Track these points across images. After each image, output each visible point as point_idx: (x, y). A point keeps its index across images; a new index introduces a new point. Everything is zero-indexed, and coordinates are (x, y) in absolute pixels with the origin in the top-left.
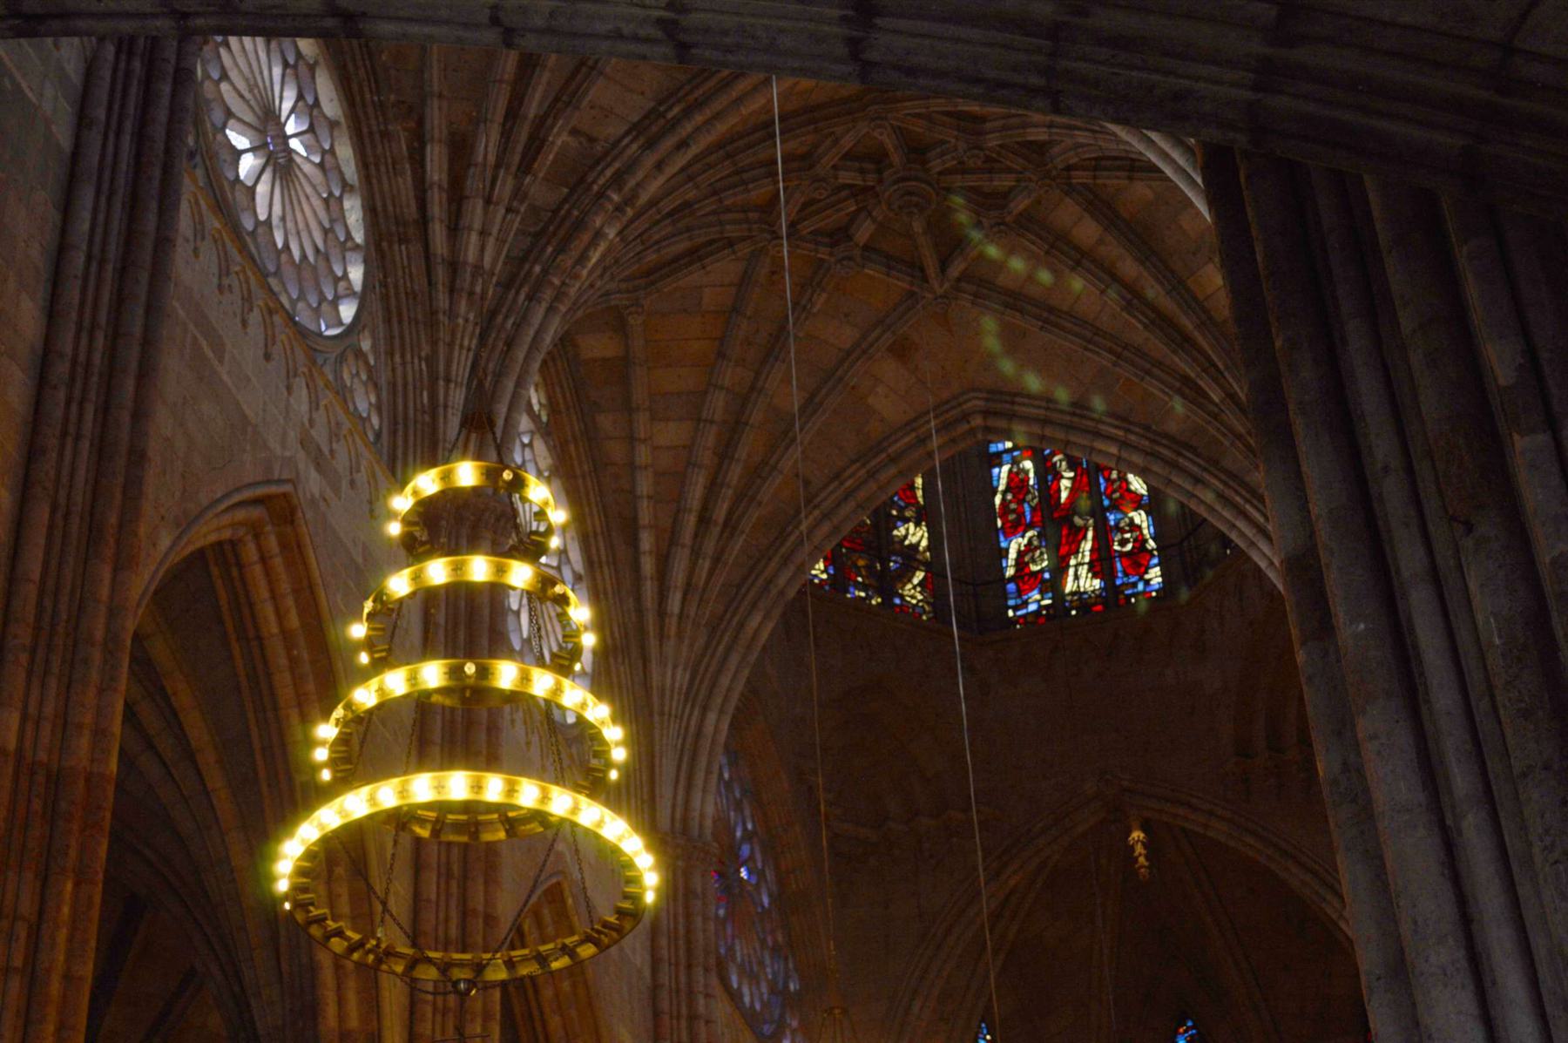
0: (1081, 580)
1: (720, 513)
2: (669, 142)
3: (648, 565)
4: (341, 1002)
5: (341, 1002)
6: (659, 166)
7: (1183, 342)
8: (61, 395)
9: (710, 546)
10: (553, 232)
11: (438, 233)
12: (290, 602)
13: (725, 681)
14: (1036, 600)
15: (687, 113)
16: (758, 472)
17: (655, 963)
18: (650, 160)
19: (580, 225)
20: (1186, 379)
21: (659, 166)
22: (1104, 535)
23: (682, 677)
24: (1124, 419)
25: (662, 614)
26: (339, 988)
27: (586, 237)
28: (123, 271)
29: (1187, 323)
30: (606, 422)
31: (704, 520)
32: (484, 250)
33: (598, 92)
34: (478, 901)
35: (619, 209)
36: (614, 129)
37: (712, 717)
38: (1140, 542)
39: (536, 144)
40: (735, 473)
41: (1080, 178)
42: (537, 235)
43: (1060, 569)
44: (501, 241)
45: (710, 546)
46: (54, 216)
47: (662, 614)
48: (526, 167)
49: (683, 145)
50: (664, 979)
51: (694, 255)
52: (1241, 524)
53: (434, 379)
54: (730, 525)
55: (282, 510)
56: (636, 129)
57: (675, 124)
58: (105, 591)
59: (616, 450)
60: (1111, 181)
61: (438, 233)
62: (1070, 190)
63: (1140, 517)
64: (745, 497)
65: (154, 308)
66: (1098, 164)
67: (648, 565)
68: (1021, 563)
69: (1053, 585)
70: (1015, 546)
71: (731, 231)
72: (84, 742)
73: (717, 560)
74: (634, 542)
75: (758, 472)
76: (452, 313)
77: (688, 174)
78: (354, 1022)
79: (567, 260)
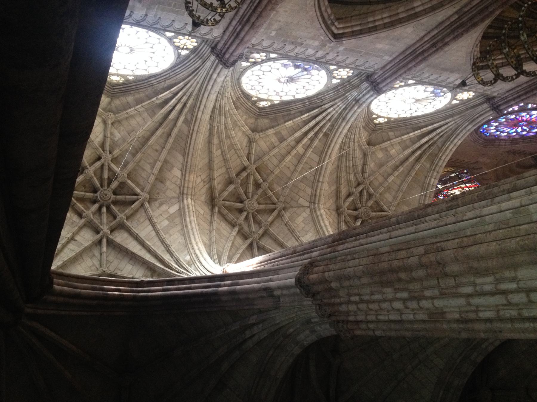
24: (426, 177)
52: (450, 147)
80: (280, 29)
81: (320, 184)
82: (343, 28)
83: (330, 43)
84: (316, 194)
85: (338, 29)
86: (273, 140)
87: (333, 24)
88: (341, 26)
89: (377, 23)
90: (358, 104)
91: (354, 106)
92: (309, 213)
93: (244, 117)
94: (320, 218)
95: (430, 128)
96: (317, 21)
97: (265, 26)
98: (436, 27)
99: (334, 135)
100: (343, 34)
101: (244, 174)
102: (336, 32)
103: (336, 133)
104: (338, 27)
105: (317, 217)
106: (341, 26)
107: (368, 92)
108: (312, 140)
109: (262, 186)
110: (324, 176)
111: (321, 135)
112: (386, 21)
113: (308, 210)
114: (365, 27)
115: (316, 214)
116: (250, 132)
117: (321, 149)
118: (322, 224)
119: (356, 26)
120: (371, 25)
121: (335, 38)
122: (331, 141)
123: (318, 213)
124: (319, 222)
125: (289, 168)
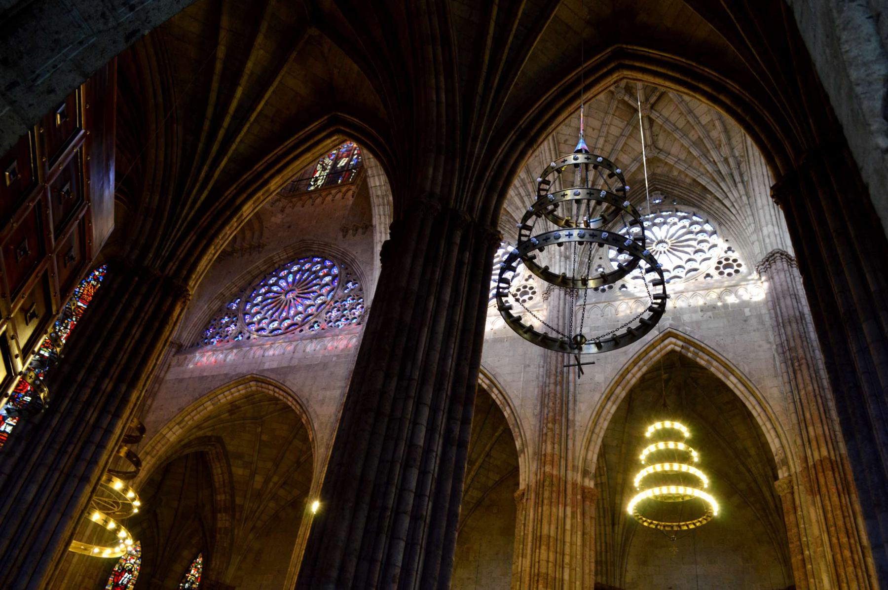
80: (745, 321)
82: (666, 346)
83: (671, 325)
85: (671, 343)
86: (625, 156)
87: (682, 347)
89: (636, 368)
90: (563, 254)
93: (676, 173)
96: (716, 348)
97: (767, 318)
98: (575, 397)
100: (663, 341)
101: (653, 100)
104: (672, 346)
109: (623, 91)
112: (630, 375)
114: (645, 359)
116: (662, 157)
119: (655, 355)
120: (641, 363)
121: (669, 332)
125: (594, 129)
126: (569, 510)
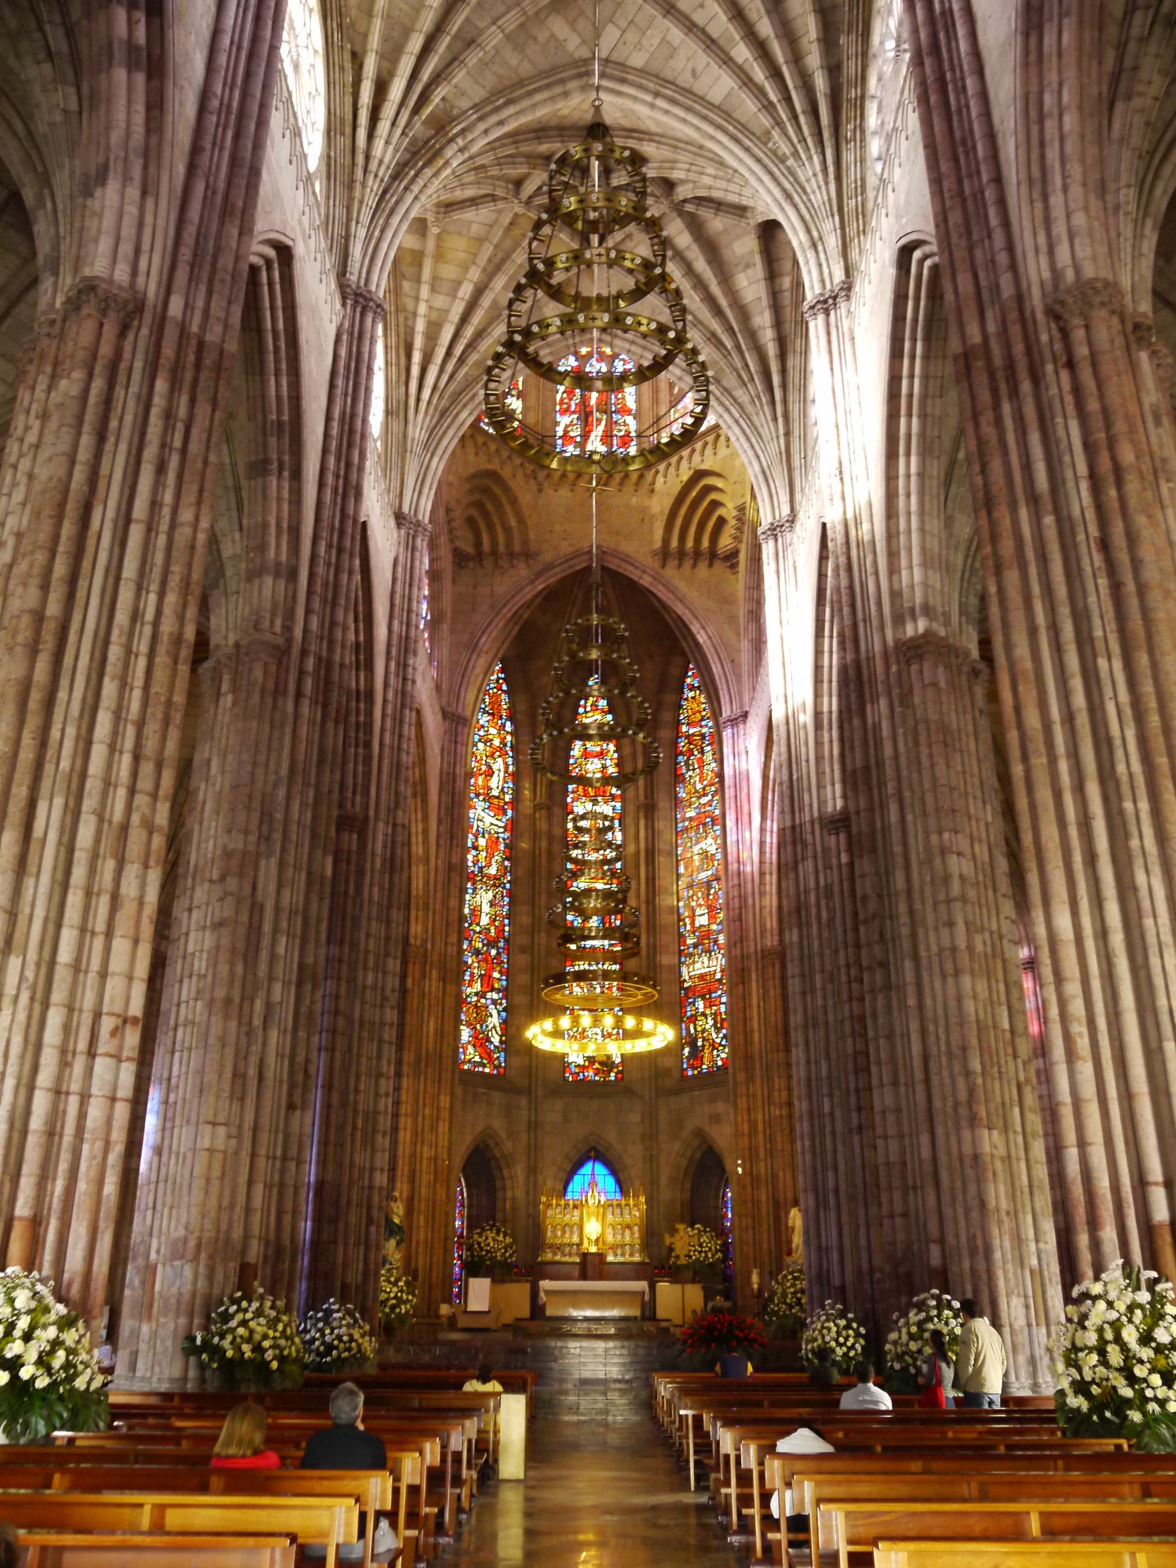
0: (595, 444)
1: (458, 351)
2: (494, 119)
3: (415, 371)
4: (278, 546)
5: (278, 546)
6: (486, 132)
7: (718, 312)
8: (214, 119)
9: (450, 368)
10: (419, 155)
11: (362, 133)
12: (280, 313)
13: (445, 442)
14: (571, 450)
15: (509, 102)
16: (479, 335)
17: (394, 579)
18: (482, 126)
19: (438, 153)
20: (714, 335)
21: (486, 132)
22: (611, 424)
23: (424, 436)
25: (418, 400)
26: (278, 537)
27: (441, 162)
28: (251, 56)
29: (723, 302)
30: (406, 286)
31: (449, 353)
32: (386, 152)
33: (460, 76)
34: (351, 511)
35: (461, 150)
36: (464, 104)
37: (435, 460)
38: (628, 433)
39: (423, 99)
40: (469, 332)
41: (689, 208)
42: (415, 154)
43: (586, 436)
44: (396, 150)
45: (450, 368)
46: (213, 9)
47: (418, 400)
48: (416, 111)
49: (501, 123)
50: (399, 588)
51: (473, 202)
53: (349, 220)
54: (461, 361)
55: (285, 253)
56: (476, 107)
57: (498, 109)
58: (234, 244)
59: (409, 303)
60: (705, 213)
61: (362, 133)
62: (681, 213)
63: (630, 420)
64: (471, 346)
65: (267, 87)
66: (700, 200)
67: (415, 371)
68: (566, 432)
69: (582, 445)
70: (564, 420)
71: (499, 192)
72: (218, 329)
73: (451, 377)
74: (409, 356)
75: (479, 335)
76: (364, 185)
77: (491, 147)
78: (284, 558)
79: (428, 172)
81: (648, 98)
84: (623, 81)
88: (925, 272)
91: (808, 231)
92: (577, 55)
94: (558, 90)
95: (776, 380)
99: (759, 161)
102: (917, 254)
103: (765, 167)
105: (562, 81)
106: (925, 272)
107: (823, 281)
108: (759, 92)
110: (667, 112)
111: (765, 121)
113: (584, 53)
115: (572, 78)
117: (736, 115)
118: (538, 97)
122: (747, 150)
123: (572, 85)
124: (547, 87)
126: (883, 702)
